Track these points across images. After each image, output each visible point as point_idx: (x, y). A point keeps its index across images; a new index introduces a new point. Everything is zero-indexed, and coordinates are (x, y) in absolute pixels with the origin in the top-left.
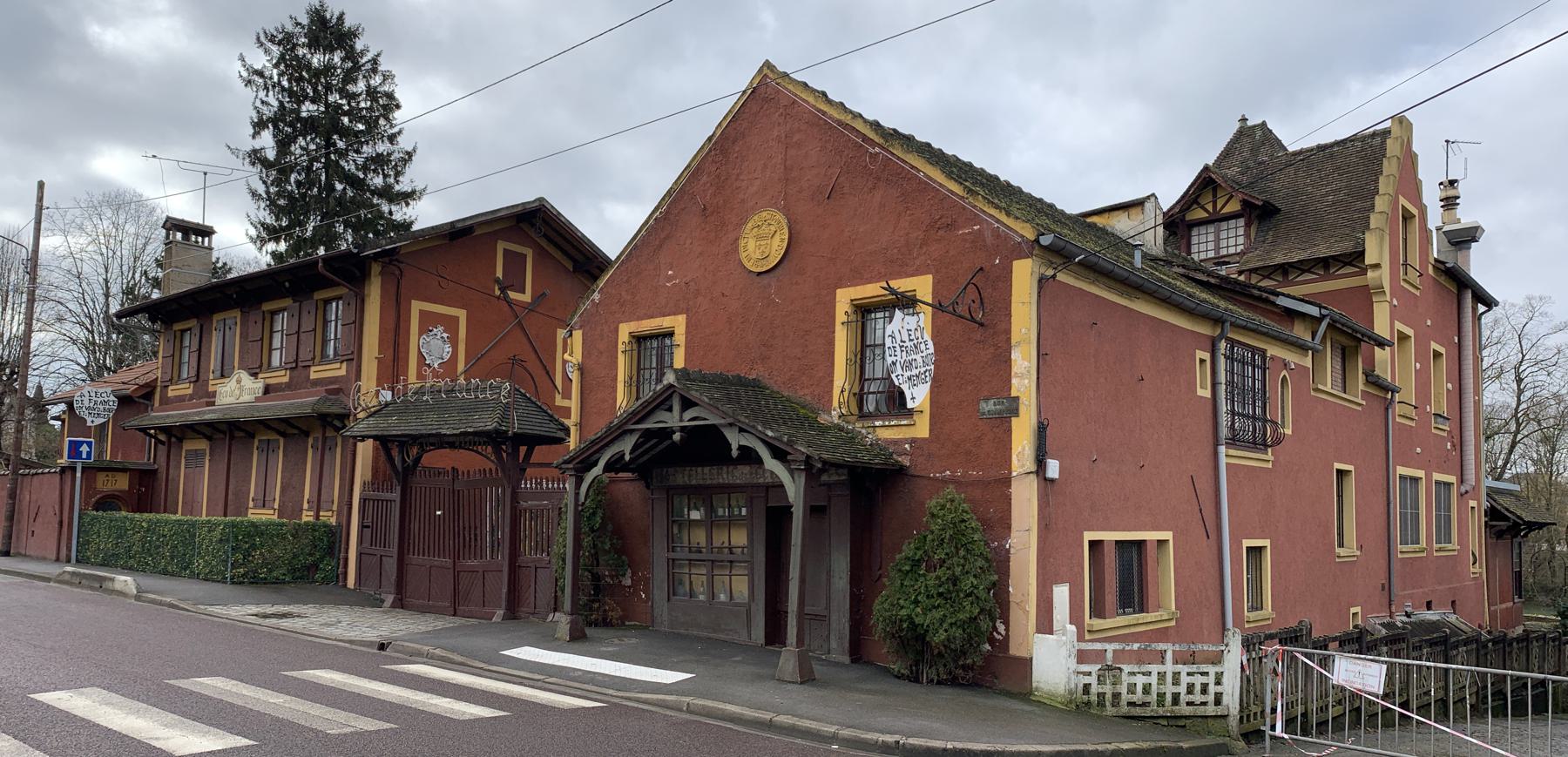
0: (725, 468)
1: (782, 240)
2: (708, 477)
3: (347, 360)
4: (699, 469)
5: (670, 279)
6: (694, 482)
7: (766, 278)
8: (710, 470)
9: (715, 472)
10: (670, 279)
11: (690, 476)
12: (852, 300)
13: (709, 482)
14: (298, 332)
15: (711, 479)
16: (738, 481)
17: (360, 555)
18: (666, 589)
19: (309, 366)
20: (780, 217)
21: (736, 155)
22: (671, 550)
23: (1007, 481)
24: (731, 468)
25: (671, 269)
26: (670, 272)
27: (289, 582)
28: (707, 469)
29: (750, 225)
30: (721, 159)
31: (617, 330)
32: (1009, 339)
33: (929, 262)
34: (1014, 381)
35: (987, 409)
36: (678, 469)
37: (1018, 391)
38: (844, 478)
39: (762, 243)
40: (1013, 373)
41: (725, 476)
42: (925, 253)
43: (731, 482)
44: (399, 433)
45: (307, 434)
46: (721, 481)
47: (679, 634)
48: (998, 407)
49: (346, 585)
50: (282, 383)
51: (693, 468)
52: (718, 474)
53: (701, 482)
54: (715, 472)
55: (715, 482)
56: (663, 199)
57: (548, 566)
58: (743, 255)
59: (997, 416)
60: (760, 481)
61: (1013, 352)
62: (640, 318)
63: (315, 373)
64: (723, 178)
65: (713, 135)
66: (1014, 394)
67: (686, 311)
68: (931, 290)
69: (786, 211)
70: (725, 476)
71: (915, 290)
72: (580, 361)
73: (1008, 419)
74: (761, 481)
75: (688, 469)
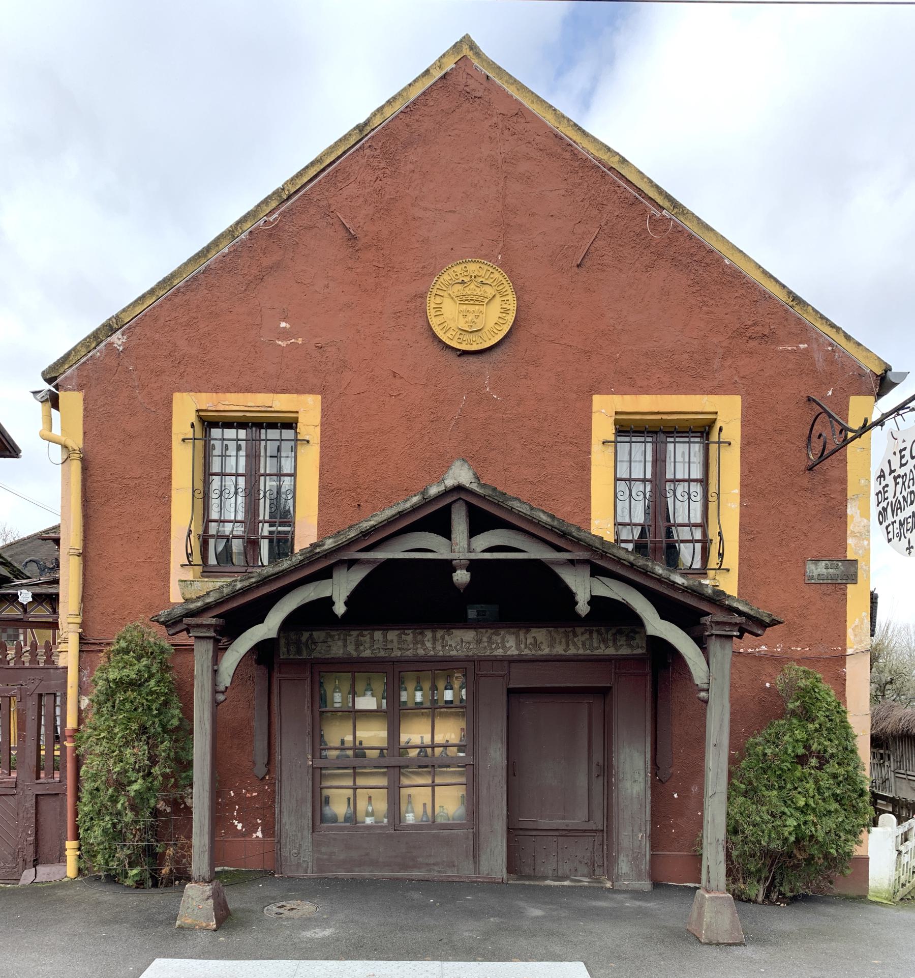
0: (429, 634)
1: (506, 311)
2: (395, 644)
4: (378, 635)
5: (285, 334)
6: (367, 653)
7: (473, 364)
8: (399, 636)
9: (410, 638)
10: (285, 334)
11: (358, 644)
12: (616, 413)
13: (397, 653)
15: (400, 649)
16: (454, 653)
18: (310, 814)
20: (498, 275)
21: (412, 167)
22: (318, 754)
23: (841, 659)
24: (440, 633)
25: (285, 319)
26: (283, 325)
28: (392, 635)
29: (446, 277)
30: (382, 165)
31: (169, 404)
32: (844, 491)
33: (736, 378)
34: (850, 541)
35: (815, 573)
36: (333, 633)
37: (856, 553)
38: (639, 651)
39: (471, 308)
40: (849, 532)
41: (429, 645)
42: (730, 367)
43: (441, 653)
46: (421, 652)
47: (336, 878)
48: (830, 571)
51: (365, 633)
52: (416, 643)
53: (382, 654)
54: (410, 638)
55: (409, 653)
56: (266, 201)
57: (14, 791)
58: (434, 322)
59: (829, 581)
60: (495, 653)
61: (849, 506)
62: (217, 389)
64: (387, 196)
65: (366, 123)
66: (850, 556)
67: (322, 390)
68: (739, 416)
69: (507, 267)
70: (429, 645)
71: (716, 413)
72: (81, 446)
73: (843, 586)
74: (499, 652)
75: (355, 633)
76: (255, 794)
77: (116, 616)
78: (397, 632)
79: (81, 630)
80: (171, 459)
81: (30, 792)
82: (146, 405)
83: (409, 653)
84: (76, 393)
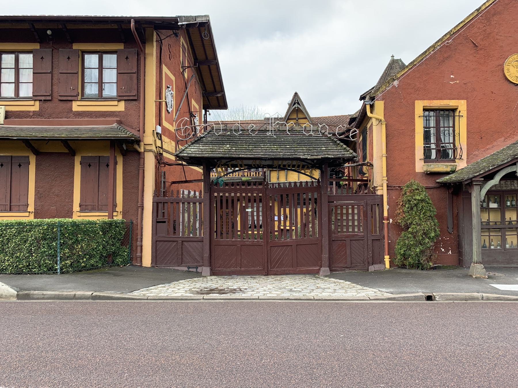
3: (125, 100)
8: (505, 182)
9: (509, 183)
13: (504, 188)
14: (51, 73)
15: (505, 187)
17: (155, 243)
19: (72, 101)
27: (100, 267)
44: (245, 156)
45: (72, 153)
46: (513, 188)
49: (142, 265)
50: (29, 112)
52: (511, 185)
54: (509, 183)
63: (76, 106)
70: (516, 185)
76: (448, 239)
77: (397, 177)
78: (505, 181)
79: (387, 182)
80: (415, 123)
81: (370, 239)
82: (406, 105)
83: (509, 188)
84: (381, 101)
